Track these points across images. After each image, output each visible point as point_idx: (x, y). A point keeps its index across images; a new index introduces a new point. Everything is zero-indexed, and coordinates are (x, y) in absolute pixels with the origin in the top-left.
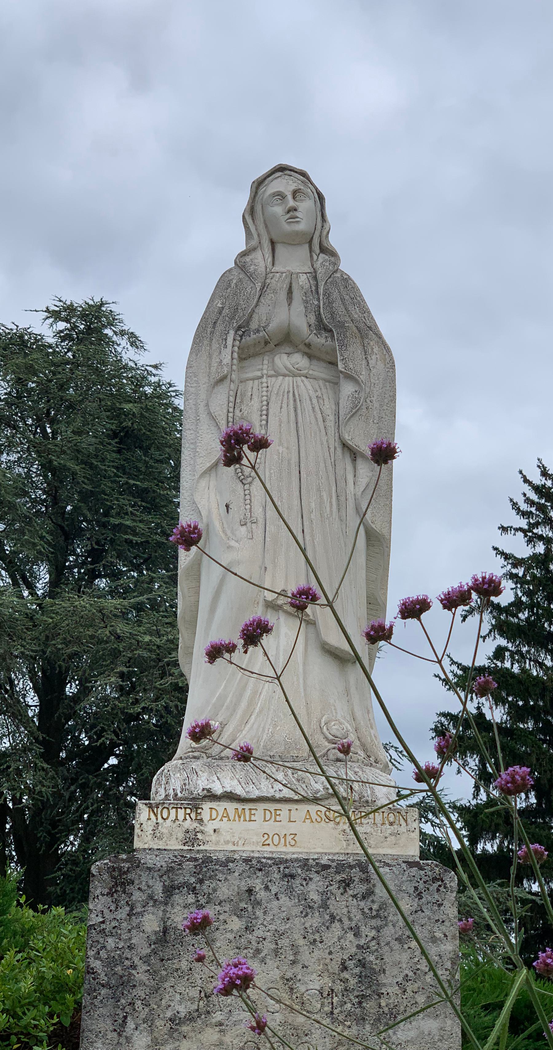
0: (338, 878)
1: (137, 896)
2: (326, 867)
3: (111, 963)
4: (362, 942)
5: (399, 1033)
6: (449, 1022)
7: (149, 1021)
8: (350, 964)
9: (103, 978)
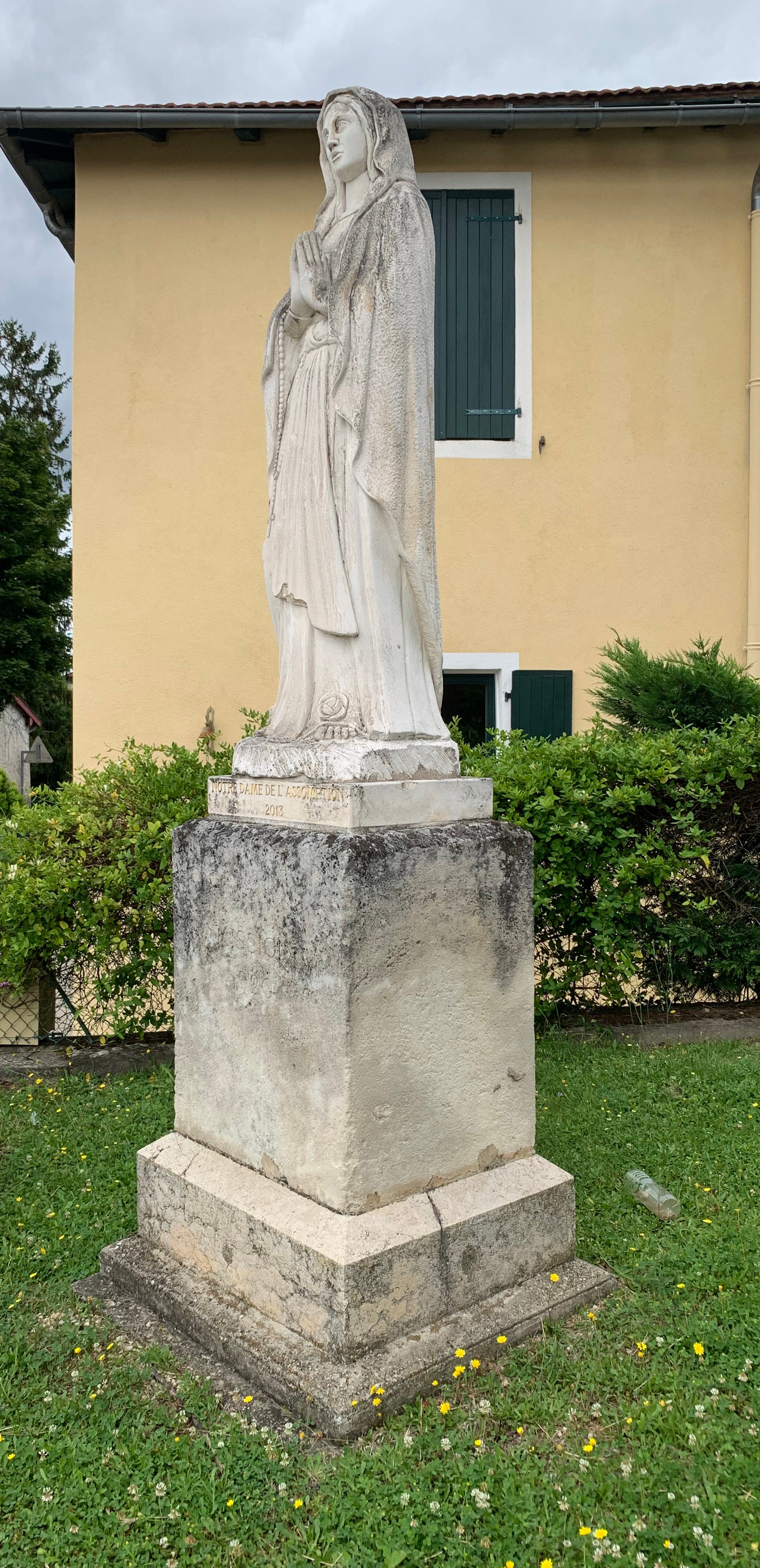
0: (281, 851)
1: (191, 855)
3: (183, 901)
5: (313, 984)
6: (340, 980)
7: (198, 946)
8: (288, 921)
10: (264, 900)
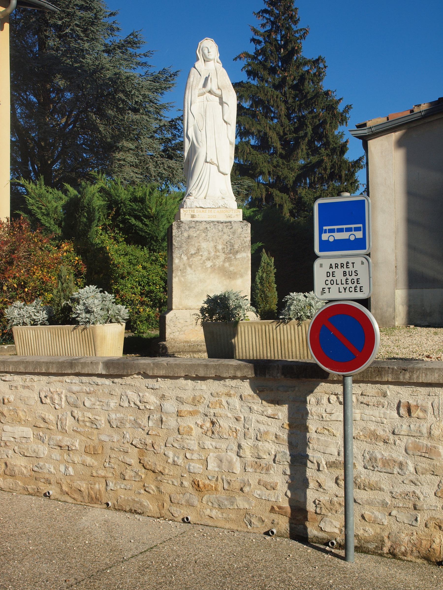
1: (183, 229)
2: (223, 223)
4: (230, 238)
9: (177, 246)
10: (217, 238)
